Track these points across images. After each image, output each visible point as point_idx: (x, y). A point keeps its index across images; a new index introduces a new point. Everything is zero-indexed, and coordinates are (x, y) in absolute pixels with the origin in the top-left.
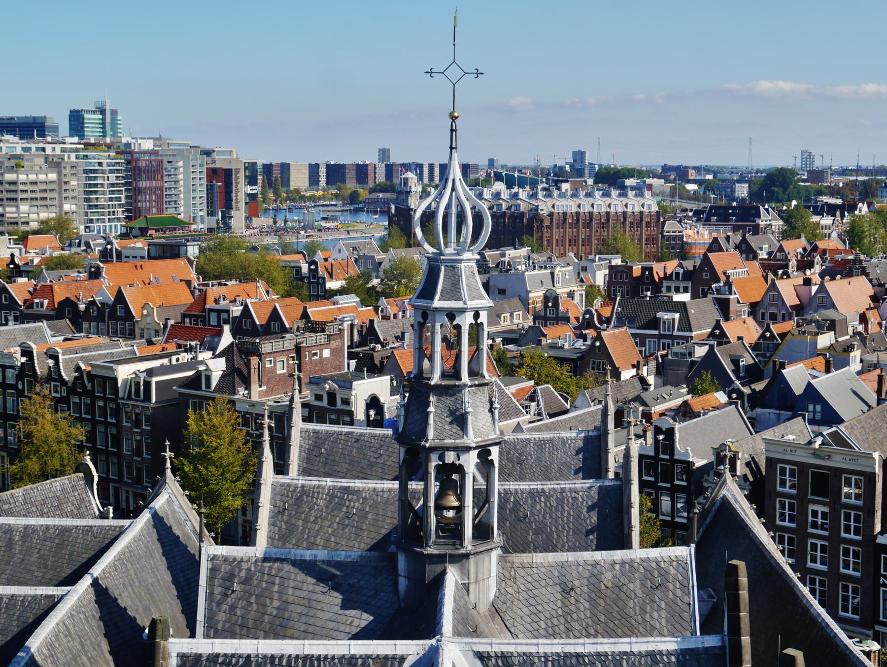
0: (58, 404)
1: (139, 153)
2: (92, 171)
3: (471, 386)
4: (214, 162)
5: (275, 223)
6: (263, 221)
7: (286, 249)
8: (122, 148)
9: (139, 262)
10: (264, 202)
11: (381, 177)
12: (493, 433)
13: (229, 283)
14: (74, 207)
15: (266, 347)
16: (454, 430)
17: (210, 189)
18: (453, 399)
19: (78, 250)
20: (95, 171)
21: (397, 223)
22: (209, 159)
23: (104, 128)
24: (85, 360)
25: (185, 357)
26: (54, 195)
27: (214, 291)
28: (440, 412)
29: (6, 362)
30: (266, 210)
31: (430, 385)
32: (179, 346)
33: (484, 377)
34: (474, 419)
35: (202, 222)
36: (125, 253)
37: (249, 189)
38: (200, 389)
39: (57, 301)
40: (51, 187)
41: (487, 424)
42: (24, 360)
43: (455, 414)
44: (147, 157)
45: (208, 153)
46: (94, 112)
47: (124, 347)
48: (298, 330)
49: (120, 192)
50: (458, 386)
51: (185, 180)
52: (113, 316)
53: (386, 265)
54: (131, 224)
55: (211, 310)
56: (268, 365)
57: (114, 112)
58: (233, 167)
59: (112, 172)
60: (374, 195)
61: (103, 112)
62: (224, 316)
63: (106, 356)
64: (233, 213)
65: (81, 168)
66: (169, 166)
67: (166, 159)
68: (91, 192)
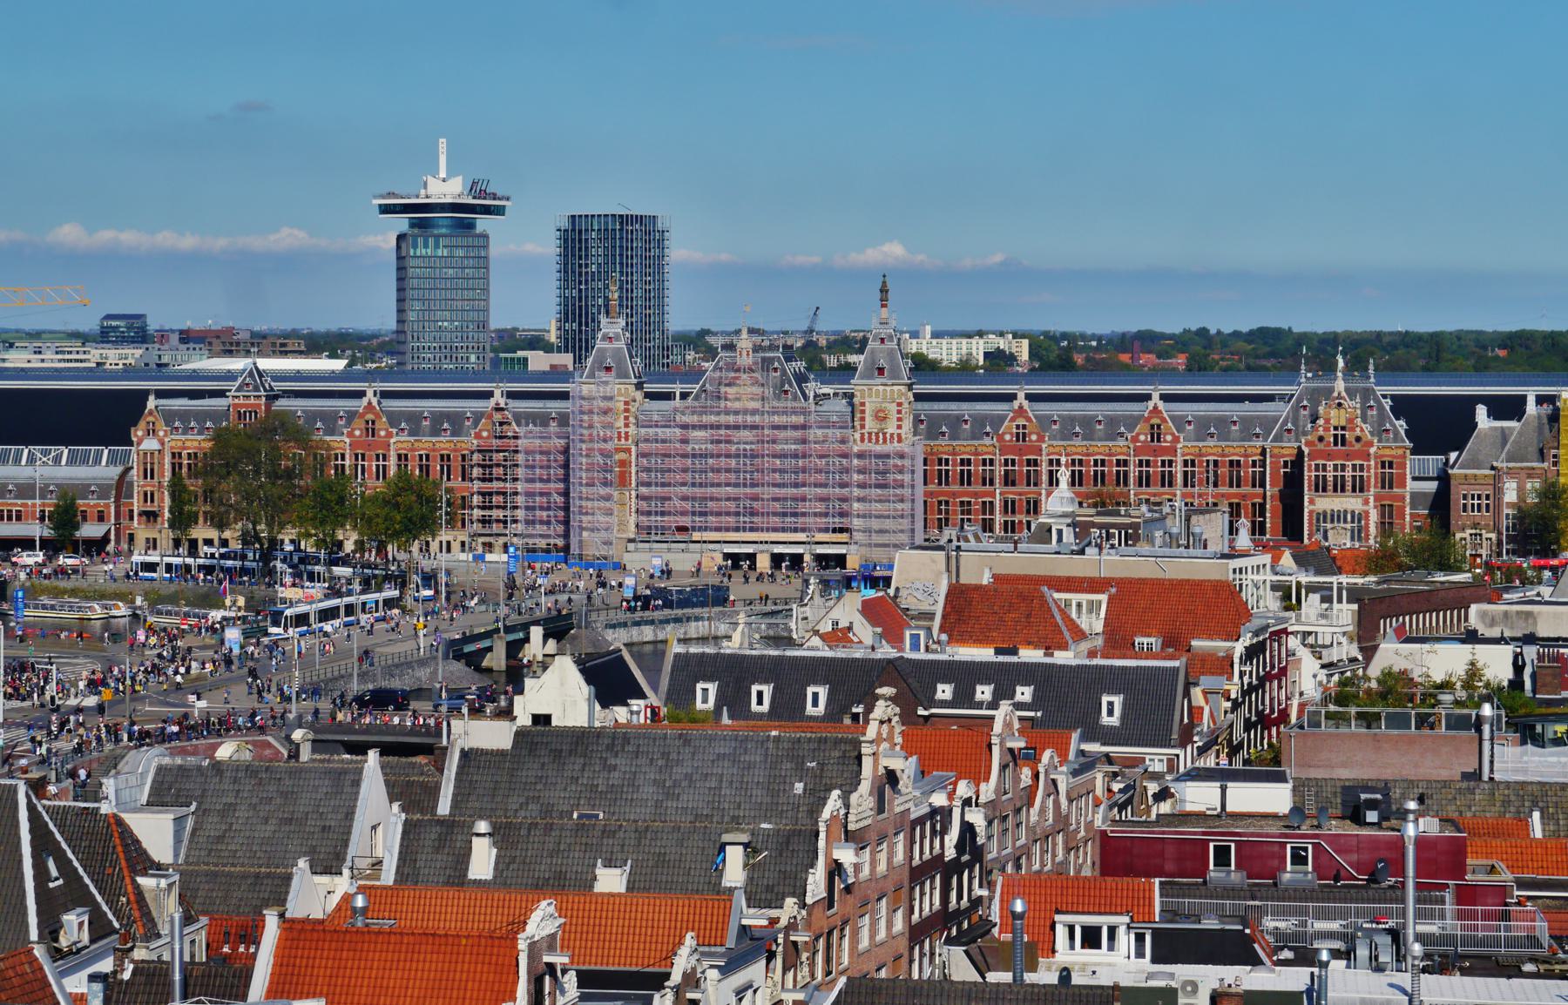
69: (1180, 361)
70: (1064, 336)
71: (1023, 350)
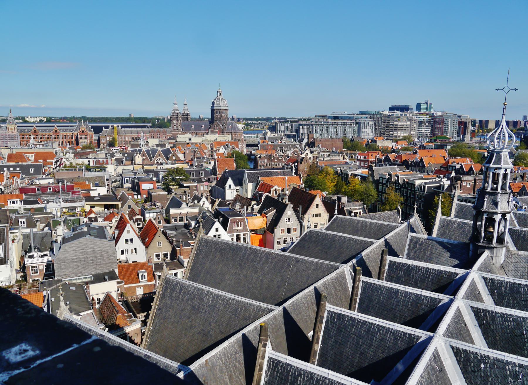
0: (397, 190)
1: (437, 116)
2: (421, 122)
4: (461, 119)
5: (480, 139)
6: (476, 139)
7: (481, 148)
8: (431, 115)
9: (429, 150)
10: (478, 133)
11: (522, 125)
13: (458, 158)
14: (414, 133)
15: (464, 178)
17: (459, 128)
19: (413, 145)
20: (422, 122)
21: (524, 141)
22: (460, 119)
23: (427, 109)
24: (406, 178)
25: (438, 180)
26: (409, 129)
27: (452, 160)
29: (384, 177)
30: (478, 136)
32: (437, 176)
35: (455, 138)
36: (426, 147)
37: (472, 128)
38: (440, 189)
39: (403, 160)
40: (408, 126)
42: (389, 176)
44: (439, 118)
45: (459, 117)
46: (424, 104)
47: (419, 175)
48: (476, 174)
49: (429, 128)
51: (451, 125)
52: (419, 166)
53: (516, 155)
54: (432, 138)
55: (450, 166)
56: (464, 184)
57: (431, 104)
58: (468, 121)
59: (427, 122)
60: (518, 131)
61: (427, 104)
62: (454, 168)
63: (413, 177)
64: (466, 136)
65: (417, 121)
66: (446, 121)
67: (445, 118)
68: (420, 128)
69: (68, 121)
70: (53, 117)
71: (45, 120)
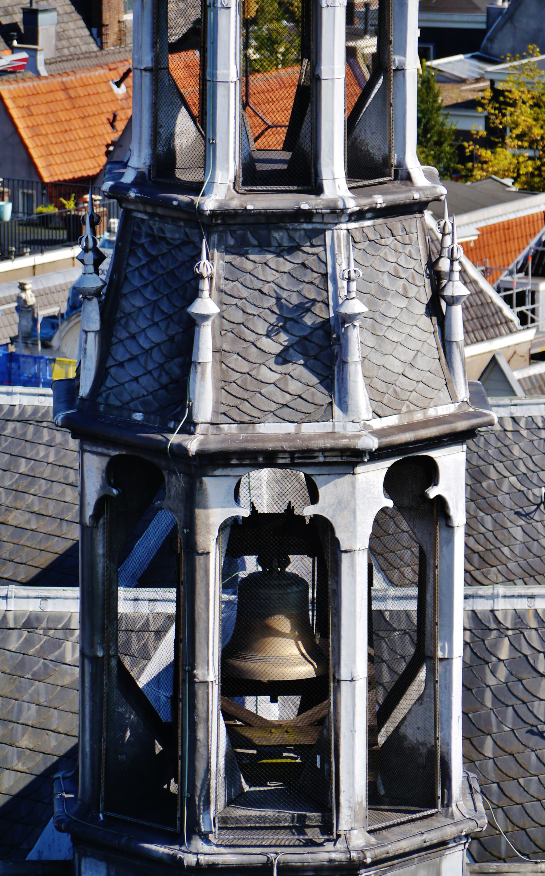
3: (359, 215)
12: (444, 394)
16: (294, 387)
18: (288, 267)
28: (239, 317)
31: (200, 211)
33: (408, 178)
34: (371, 341)
41: (421, 363)
43: (297, 321)
50: (308, 215)
